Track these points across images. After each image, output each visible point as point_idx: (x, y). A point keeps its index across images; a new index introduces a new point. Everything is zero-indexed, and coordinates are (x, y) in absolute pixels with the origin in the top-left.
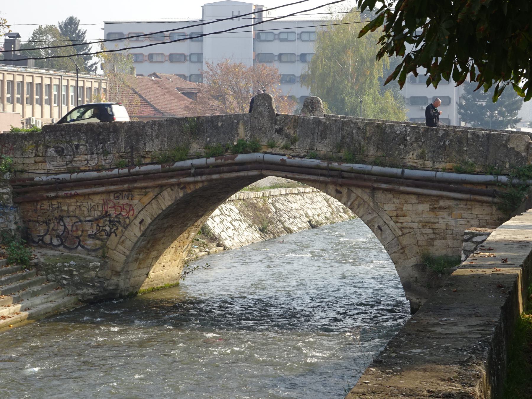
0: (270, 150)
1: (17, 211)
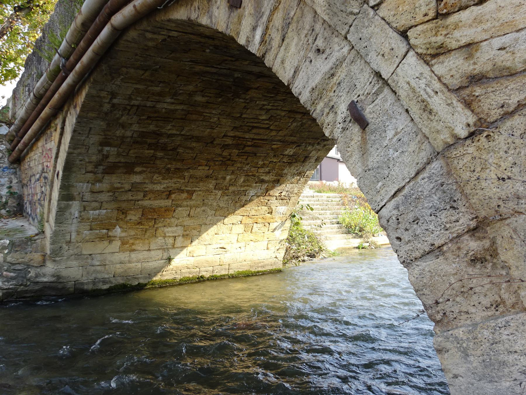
1: (15, 173)
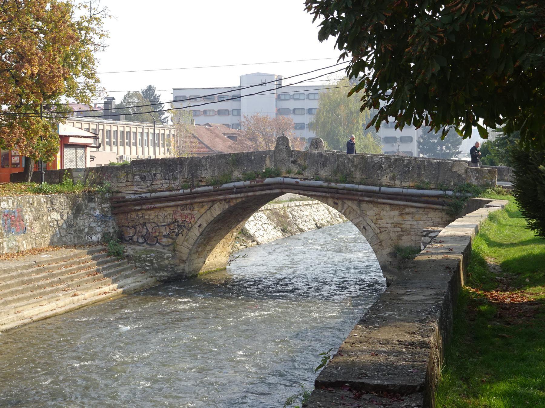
0: (288, 175)
1: (114, 220)
